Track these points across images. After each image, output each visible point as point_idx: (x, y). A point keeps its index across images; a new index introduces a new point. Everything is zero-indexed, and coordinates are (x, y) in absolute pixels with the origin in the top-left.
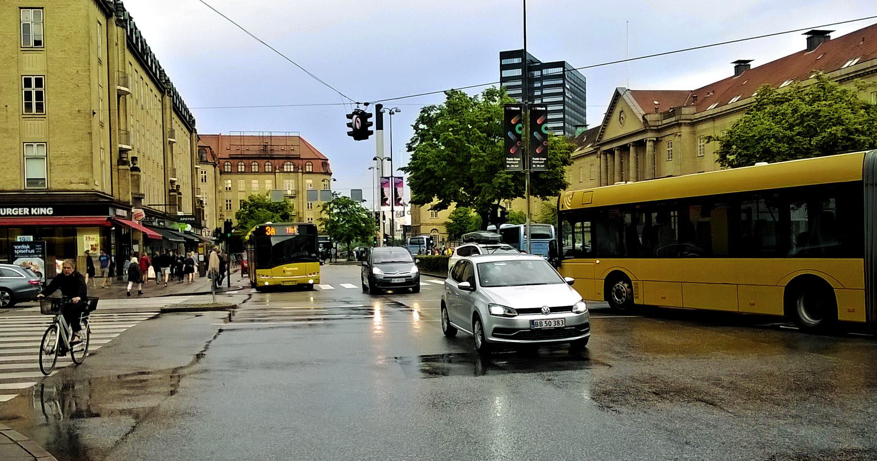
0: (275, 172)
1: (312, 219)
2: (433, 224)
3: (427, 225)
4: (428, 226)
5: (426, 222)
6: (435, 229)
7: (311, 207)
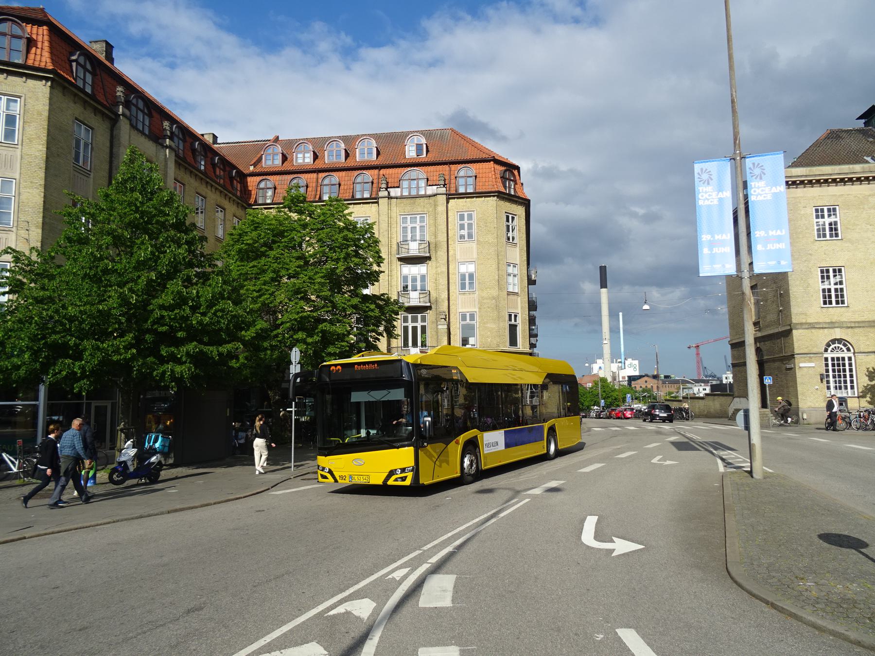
0: (377, 198)
1: (472, 317)
2: (832, 325)
3: (812, 326)
4: (813, 330)
5: (810, 320)
6: (840, 341)
7: (471, 284)
